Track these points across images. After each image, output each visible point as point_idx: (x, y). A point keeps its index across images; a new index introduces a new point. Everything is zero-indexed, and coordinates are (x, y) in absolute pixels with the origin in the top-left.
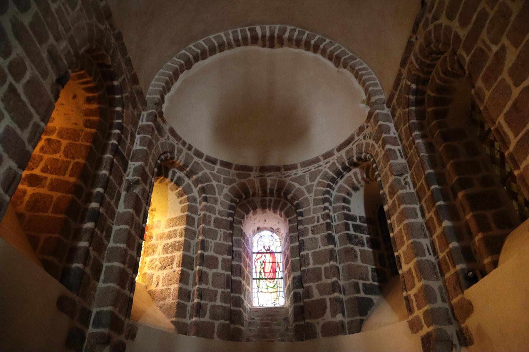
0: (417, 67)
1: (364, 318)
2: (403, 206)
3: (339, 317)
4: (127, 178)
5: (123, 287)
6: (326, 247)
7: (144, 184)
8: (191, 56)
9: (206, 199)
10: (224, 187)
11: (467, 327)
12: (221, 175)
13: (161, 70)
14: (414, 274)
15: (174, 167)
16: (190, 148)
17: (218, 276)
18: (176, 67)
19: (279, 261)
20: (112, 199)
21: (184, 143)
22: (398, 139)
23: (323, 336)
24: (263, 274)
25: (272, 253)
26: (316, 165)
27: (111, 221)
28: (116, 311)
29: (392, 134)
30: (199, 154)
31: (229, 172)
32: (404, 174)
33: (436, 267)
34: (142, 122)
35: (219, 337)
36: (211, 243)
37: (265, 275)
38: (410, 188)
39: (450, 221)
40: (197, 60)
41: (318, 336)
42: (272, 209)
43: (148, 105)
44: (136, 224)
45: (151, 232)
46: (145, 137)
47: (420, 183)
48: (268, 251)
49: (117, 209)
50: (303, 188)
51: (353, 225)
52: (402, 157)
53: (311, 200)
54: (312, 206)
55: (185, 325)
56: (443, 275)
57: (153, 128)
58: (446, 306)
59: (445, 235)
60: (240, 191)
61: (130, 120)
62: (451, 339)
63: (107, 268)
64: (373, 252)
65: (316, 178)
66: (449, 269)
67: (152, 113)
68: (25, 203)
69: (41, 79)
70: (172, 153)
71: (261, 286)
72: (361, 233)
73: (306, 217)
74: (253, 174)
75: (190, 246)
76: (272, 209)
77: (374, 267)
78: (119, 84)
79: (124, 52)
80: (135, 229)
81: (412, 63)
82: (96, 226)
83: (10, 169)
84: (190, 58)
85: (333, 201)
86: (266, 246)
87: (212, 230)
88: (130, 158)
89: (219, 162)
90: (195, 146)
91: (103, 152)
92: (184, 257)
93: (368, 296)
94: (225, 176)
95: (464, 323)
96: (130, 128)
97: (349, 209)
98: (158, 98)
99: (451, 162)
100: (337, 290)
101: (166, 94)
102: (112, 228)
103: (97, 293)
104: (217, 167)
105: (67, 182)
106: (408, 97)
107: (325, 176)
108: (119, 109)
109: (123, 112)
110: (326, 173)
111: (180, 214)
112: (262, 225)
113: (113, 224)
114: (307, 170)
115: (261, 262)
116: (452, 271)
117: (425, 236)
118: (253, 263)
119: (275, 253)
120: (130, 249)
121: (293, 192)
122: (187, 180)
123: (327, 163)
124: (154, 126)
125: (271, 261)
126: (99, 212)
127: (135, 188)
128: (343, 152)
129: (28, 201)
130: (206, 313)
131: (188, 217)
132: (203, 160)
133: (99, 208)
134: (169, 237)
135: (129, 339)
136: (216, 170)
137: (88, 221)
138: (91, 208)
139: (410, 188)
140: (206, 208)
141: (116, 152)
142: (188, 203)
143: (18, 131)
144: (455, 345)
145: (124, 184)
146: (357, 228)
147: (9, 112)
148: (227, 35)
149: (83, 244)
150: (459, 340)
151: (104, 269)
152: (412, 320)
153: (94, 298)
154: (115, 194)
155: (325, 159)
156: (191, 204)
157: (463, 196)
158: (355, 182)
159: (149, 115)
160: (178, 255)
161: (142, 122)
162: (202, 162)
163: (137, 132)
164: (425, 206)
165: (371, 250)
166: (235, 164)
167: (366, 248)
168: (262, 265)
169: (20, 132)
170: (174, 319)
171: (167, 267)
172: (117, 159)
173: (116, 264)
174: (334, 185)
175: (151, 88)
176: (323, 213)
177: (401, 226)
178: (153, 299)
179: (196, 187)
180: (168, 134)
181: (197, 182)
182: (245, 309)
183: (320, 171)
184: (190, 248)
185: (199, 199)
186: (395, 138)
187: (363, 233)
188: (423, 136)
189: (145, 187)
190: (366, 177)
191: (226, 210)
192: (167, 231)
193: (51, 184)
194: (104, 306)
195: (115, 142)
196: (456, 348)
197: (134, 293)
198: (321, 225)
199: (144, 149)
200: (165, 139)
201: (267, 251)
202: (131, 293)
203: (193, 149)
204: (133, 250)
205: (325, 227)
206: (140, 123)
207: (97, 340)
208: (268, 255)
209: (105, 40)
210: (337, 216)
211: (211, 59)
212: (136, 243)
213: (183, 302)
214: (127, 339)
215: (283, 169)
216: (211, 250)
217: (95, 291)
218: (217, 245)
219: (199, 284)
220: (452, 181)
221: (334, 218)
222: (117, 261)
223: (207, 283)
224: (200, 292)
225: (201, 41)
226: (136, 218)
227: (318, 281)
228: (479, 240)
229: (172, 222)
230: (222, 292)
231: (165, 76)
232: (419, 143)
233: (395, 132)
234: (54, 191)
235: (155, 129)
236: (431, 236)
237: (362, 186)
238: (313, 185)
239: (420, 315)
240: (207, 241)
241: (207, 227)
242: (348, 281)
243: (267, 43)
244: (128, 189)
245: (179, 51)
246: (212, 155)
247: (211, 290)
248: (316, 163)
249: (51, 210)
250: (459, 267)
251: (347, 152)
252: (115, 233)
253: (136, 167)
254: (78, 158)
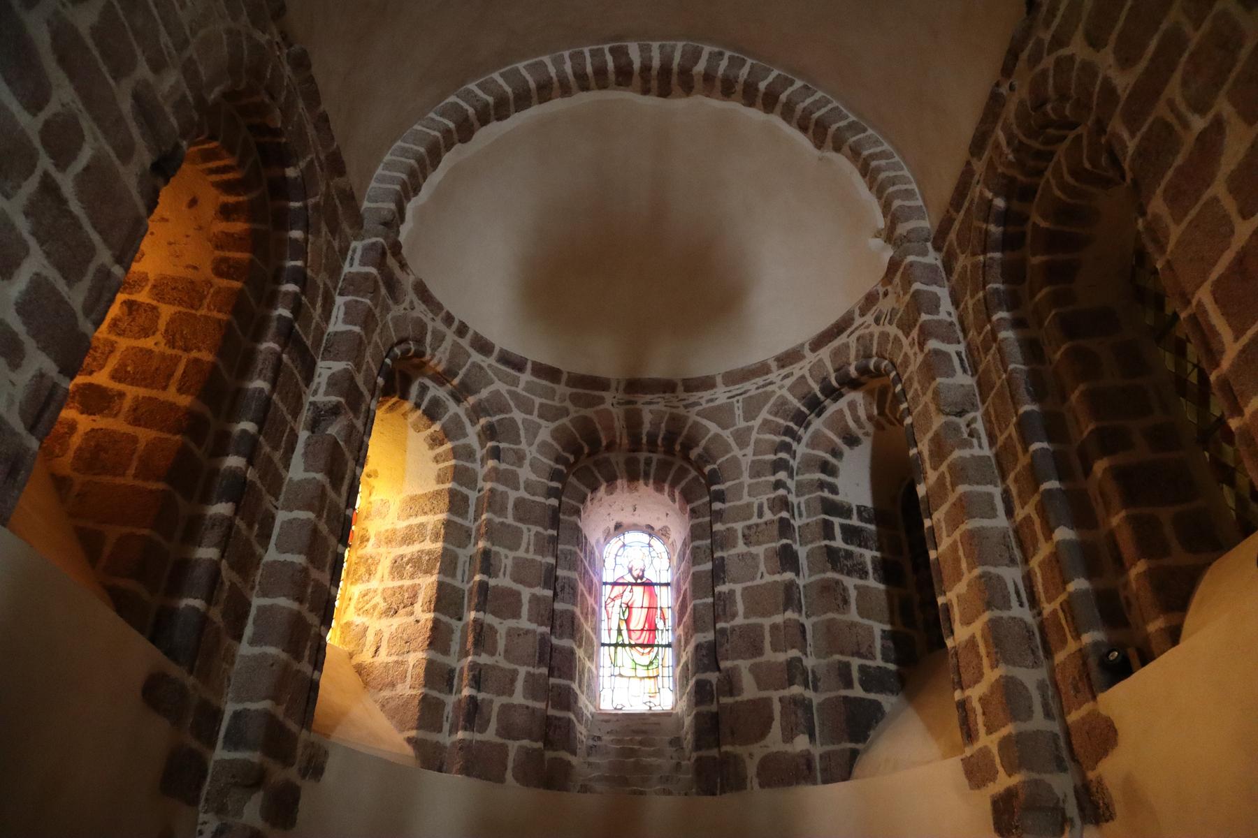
0: (1011, 157)
1: (859, 746)
2: (962, 488)
3: (801, 743)
4: (312, 399)
5: (298, 656)
6: (777, 577)
7: (351, 415)
8: (471, 111)
9: (496, 454)
10: (540, 426)
11: (1101, 780)
12: (533, 397)
13: (399, 143)
14: (982, 650)
15: (424, 375)
16: (462, 330)
17: (519, 635)
18: (434, 136)
19: (665, 605)
20: (275, 448)
21: (449, 319)
22: (958, 327)
23: (762, 786)
24: (625, 633)
25: (648, 585)
26: (760, 381)
27: (273, 499)
28: (280, 712)
29: (943, 316)
30: (484, 346)
31: (554, 391)
32: (968, 412)
33: (1034, 634)
34: (351, 265)
35: (517, 779)
36: (506, 558)
37: (630, 637)
38: (980, 446)
39: (1072, 529)
40: (484, 121)
41: (749, 786)
42: (651, 481)
43: (367, 225)
44: (329, 510)
45: (364, 527)
46: (357, 301)
47: (1006, 435)
48: (639, 581)
49: (288, 471)
50: (727, 434)
51: (842, 526)
52: (965, 371)
53: (745, 463)
54: (746, 479)
55: (438, 747)
56: (1049, 654)
57: (376, 282)
58: (1055, 727)
59: (1058, 561)
60: (578, 436)
61: (323, 261)
62: (1061, 804)
63: (262, 609)
64: (888, 592)
65: (760, 409)
66: (1064, 642)
67: (374, 244)
68: (71, 453)
69: (117, 162)
70: (420, 341)
71: (619, 663)
72: (860, 546)
73: (731, 504)
74: (608, 396)
75: (456, 564)
76: (651, 481)
77: (887, 627)
78: (300, 174)
79: (313, 98)
80: (328, 522)
81: (997, 146)
82: (236, 512)
83: (41, 375)
84: (468, 116)
85: (799, 468)
86: (634, 569)
87: (509, 526)
88: (321, 352)
89: (529, 366)
90: (475, 326)
91: (258, 337)
92: (441, 586)
93: (872, 696)
94: (544, 401)
95: (1093, 769)
96: (322, 279)
97: (834, 489)
98: (390, 210)
99: (1082, 387)
100: (799, 678)
101: (409, 200)
102: (273, 518)
103: (237, 666)
104: (526, 377)
105: (172, 407)
106: (986, 229)
107: (781, 408)
108: (296, 234)
109: (306, 240)
110: (783, 402)
111: (434, 487)
112: (626, 518)
113: (277, 508)
114: (739, 392)
115: (621, 606)
116: (1072, 646)
117: (1012, 562)
118: (603, 608)
119: (656, 584)
120: (314, 567)
121: (703, 443)
122: (453, 408)
123: (786, 377)
124: (379, 276)
125: (646, 604)
126: (245, 478)
127: (332, 424)
128: (825, 353)
129: (80, 449)
130: (488, 721)
131: (452, 494)
132: (492, 360)
133: (244, 469)
134: (408, 539)
135: (307, 778)
136: (522, 385)
137: (220, 500)
138: (225, 470)
139: (980, 446)
140: (496, 475)
141: (288, 336)
142: (453, 462)
143: (61, 286)
144: (1072, 820)
145: (305, 414)
146: (851, 534)
147: (42, 243)
148: (558, 62)
149: (206, 553)
150: (1081, 809)
151: (253, 612)
152: (972, 756)
153: (229, 680)
154: (283, 437)
155: (783, 367)
156: (461, 463)
157: (1105, 470)
158: (851, 424)
159: (366, 250)
160: (427, 583)
161: (351, 265)
162: (490, 366)
163: (338, 291)
164: (1014, 491)
165: (882, 587)
166: (568, 373)
167: (872, 583)
168: (624, 613)
169: (66, 289)
170: (413, 733)
171: (401, 612)
172: (289, 353)
173: (283, 602)
174: (801, 431)
175: (373, 184)
176: (772, 496)
177: (957, 535)
178: (366, 684)
179: (473, 423)
180: (411, 296)
181: (477, 412)
182: (580, 715)
183: (768, 396)
184: (455, 568)
185: (479, 453)
186: (951, 324)
187: (866, 547)
188: (1017, 324)
189: (355, 421)
190: (880, 414)
191: (543, 480)
192: (402, 524)
193: (135, 410)
194: (251, 700)
195: (286, 313)
196: (1073, 826)
197: (321, 671)
198: (766, 523)
199: (355, 332)
200: (405, 309)
201: (636, 579)
202: (314, 670)
203: (471, 333)
204: (323, 571)
205: (775, 530)
206: (346, 269)
207: (233, 777)
208: (639, 590)
209: (269, 71)
210: (805, 503)
211: (517, 120)
212: (329, 553)
213: (435, 693)
214: (304, 776)
215: (680, 388)
216: (504, 574)
217: (233, 663)
218: (519, 564)
219: (476, 654)
220: (1082, 433)
221: (799, 507)
222: (284, 596)
223: (492, 654)
224: (477, 673)
225: (496, 76)
226: (331, 494)
227: (753, 656)
228: (1139, 575)
229: (415, 504)
230: (528, 673)
231: (409, 158)
232: (1006, 339)
233: (952, 309)
234: (140, 425)
235: (381, 283)
236: (1026, 561)
237: (867, 434)
238: (750, 429)
239: (989, 744)
240: (497, 553)
241: (497, 520)
242: (824, 658)
243: (654, 84)
244: (314, 426)
245: (444, 95)
246: (516, 348)
247: (502, 670)
248: (759, 376)
249: (133, 472)
250: (1087, 638)
251: (836, 354)
252: (281, 528)
253: (333, 374)
254: (199, 350)
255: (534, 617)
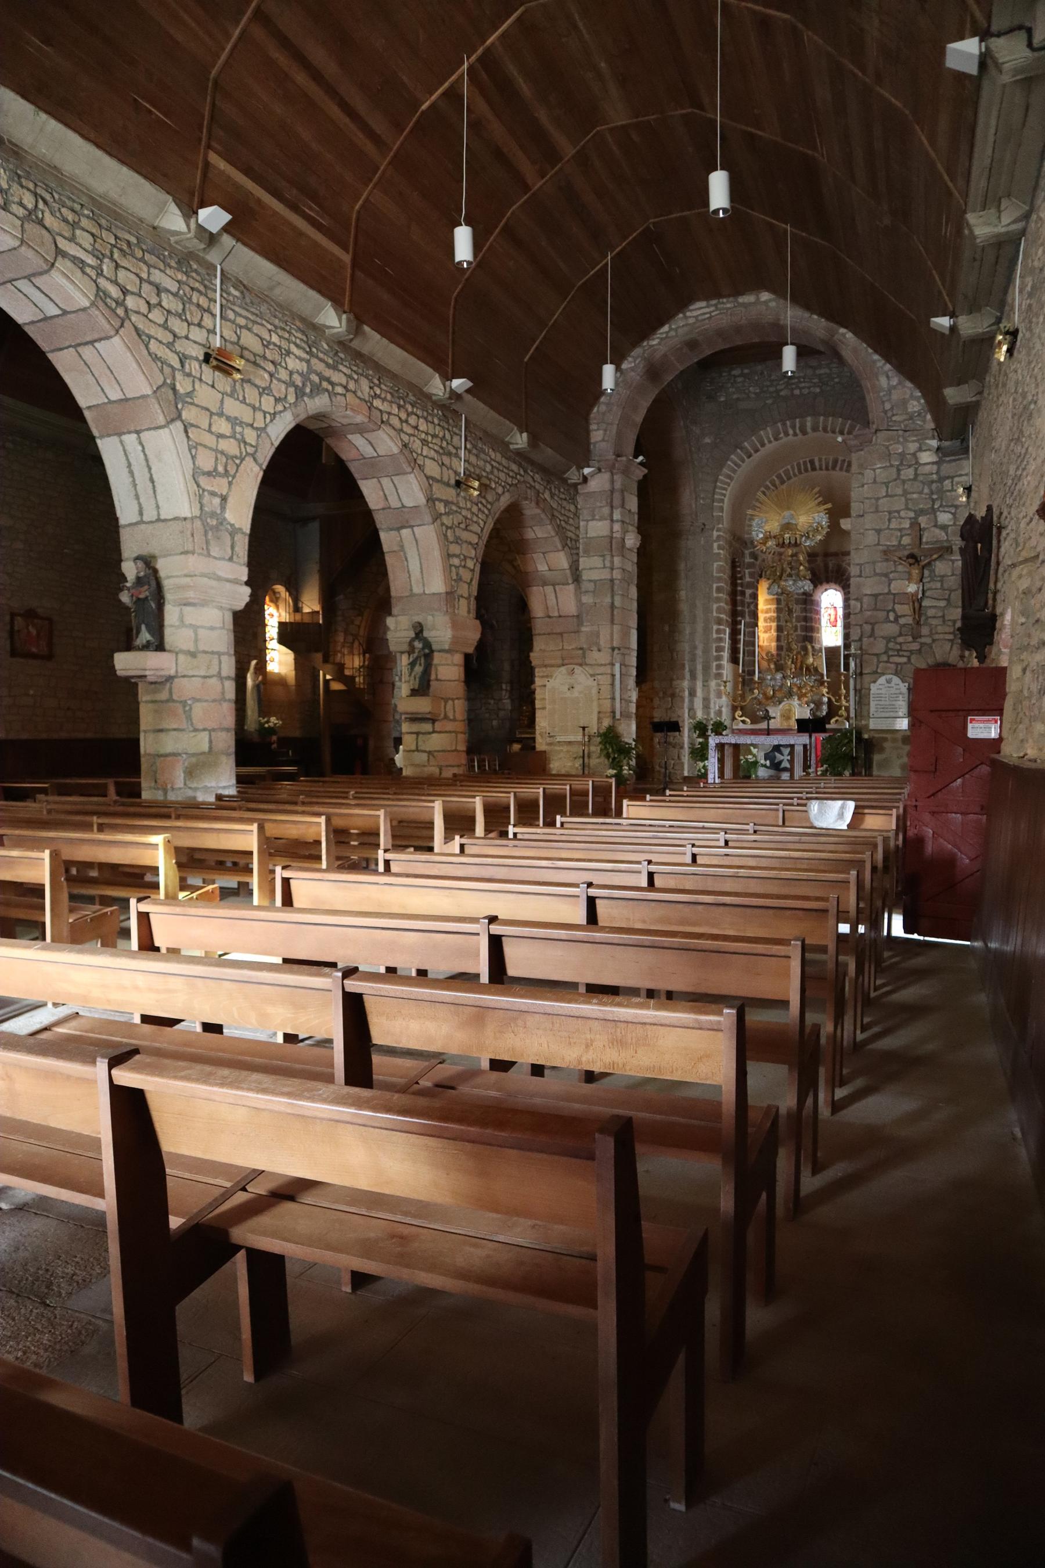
160: (774, 625)
255: (802, 631)
